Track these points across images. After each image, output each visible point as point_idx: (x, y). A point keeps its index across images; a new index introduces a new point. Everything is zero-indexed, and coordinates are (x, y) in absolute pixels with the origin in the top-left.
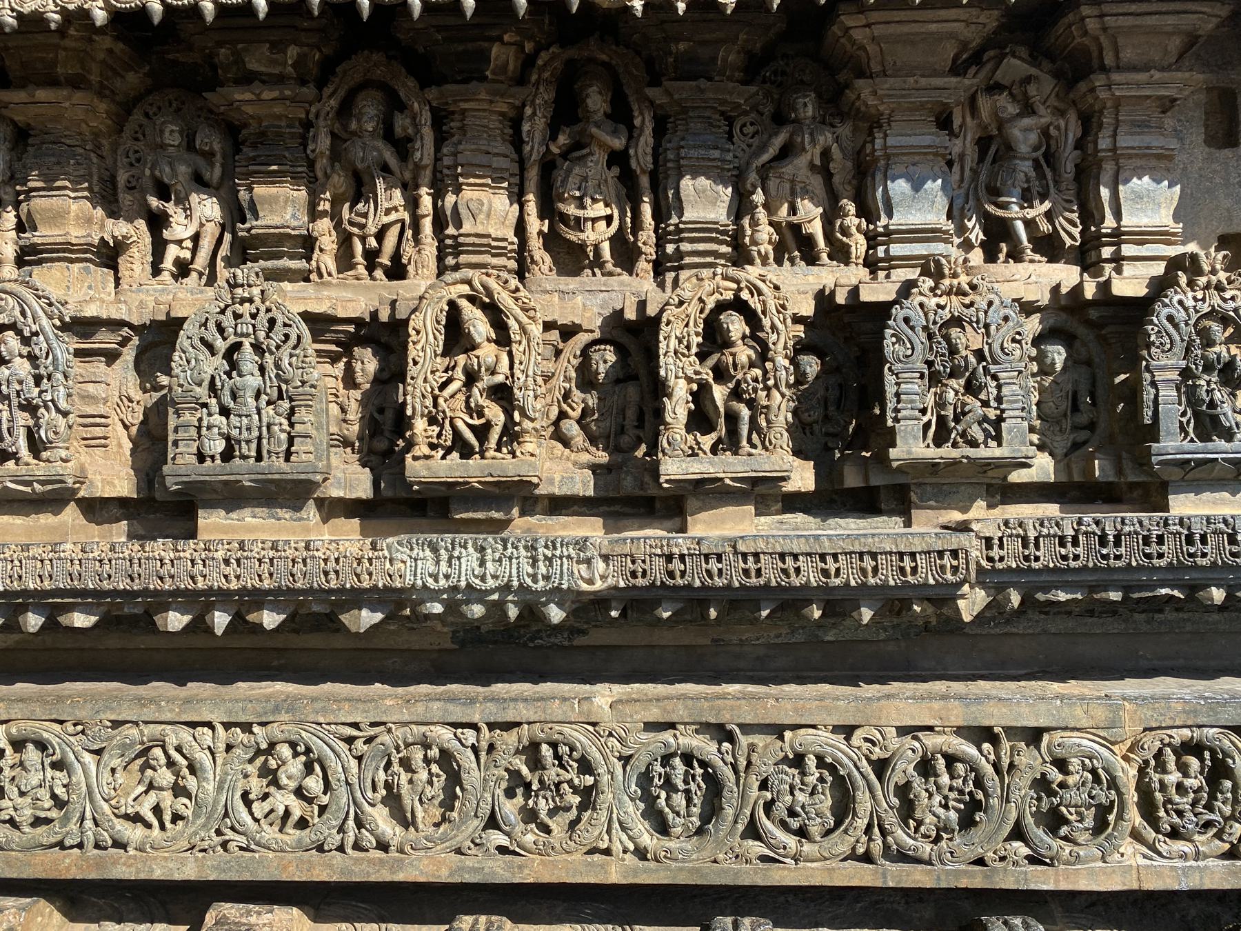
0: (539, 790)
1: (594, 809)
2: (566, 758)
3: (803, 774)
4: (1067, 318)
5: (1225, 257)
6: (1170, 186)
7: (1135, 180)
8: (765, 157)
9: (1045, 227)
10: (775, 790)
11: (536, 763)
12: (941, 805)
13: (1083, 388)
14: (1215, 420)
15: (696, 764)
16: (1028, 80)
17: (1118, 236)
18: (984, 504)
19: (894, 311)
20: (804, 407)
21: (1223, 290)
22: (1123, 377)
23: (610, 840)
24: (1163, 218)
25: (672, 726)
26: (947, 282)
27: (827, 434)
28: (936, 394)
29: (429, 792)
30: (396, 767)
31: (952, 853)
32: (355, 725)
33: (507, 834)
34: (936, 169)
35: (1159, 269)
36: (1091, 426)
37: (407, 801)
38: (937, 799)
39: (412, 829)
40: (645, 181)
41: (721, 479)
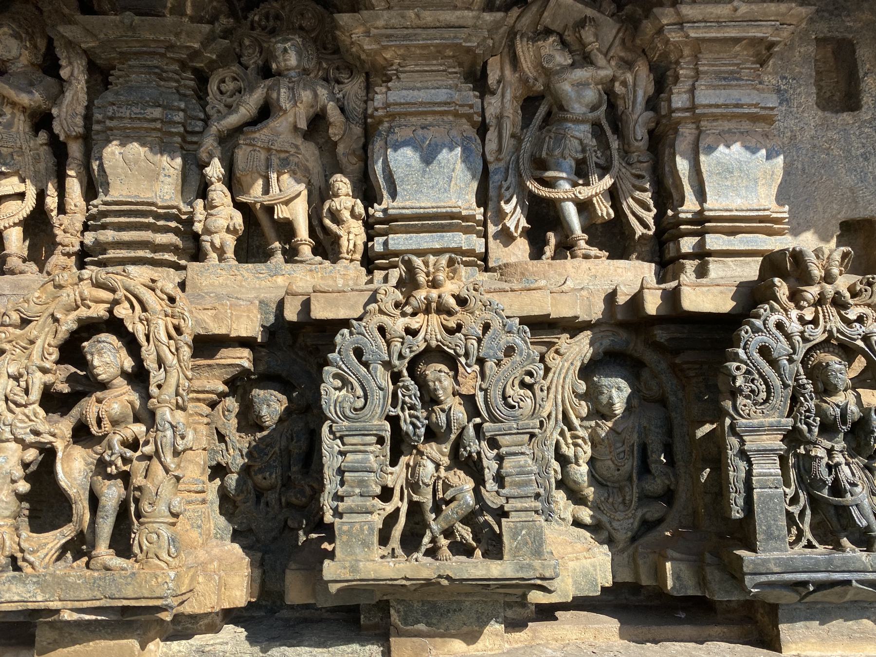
4: (630, 339)
5: (845, 256)
6: (769, 157)
7: (722, 148)
8: (233, 120)
9: (604, 210)
13: (655, 441)
14: (843, 511)
16: (582, 23)
17: (701, 223)
18: (500, 627)
19: (338, 339)
20: (257, 465)
21: (845, 306)
22: (708, 428)
24: (763, 198)
26: (421, 294)
27: (289, 505)
28: (408, 465)
34: (454, 133)
35: (751, 270)
36: (668, 496)
40: (75, 149)
41: (57, 611)
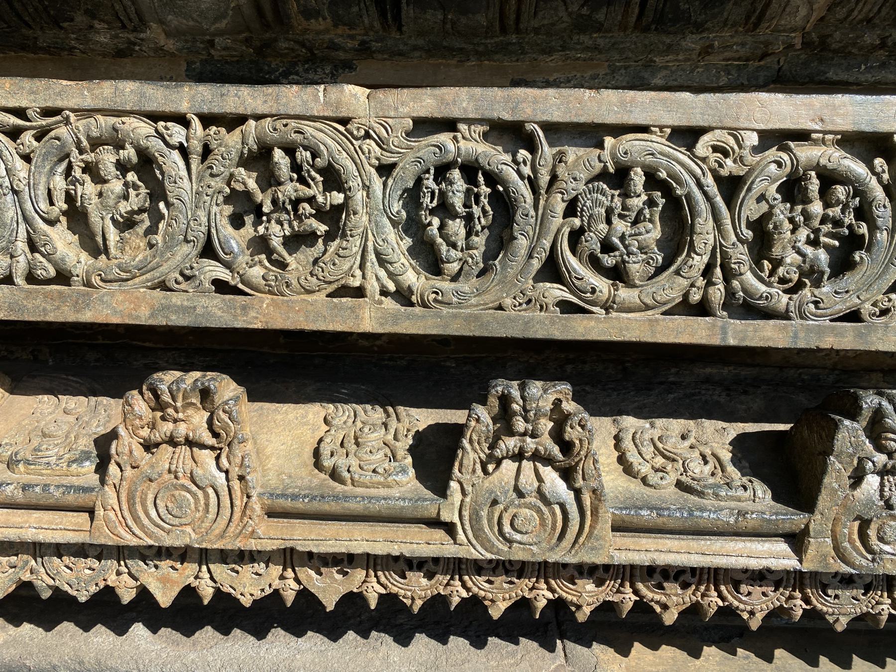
0: (272, 212)
1: (344, 236)
2: (306, 167)
3: (626, 195)
10: (586, 214)
11: (269, 180)
12: (809, 242)
15: (481, 179)
23: (364, 277)
25: (449, 125)
29: (124, 207)
30: (77, 173)
31: (816, 303)
32: (20, 112)
33: (228, 266)
37: (94, 218)
38: (803, 233)
39: (103, 257)
